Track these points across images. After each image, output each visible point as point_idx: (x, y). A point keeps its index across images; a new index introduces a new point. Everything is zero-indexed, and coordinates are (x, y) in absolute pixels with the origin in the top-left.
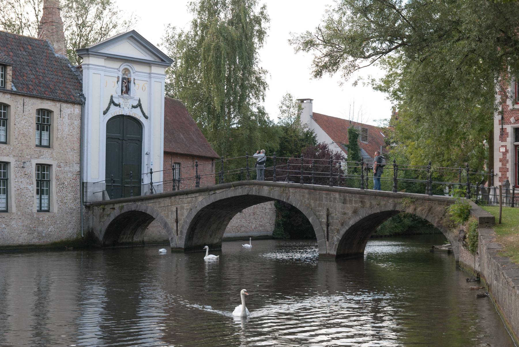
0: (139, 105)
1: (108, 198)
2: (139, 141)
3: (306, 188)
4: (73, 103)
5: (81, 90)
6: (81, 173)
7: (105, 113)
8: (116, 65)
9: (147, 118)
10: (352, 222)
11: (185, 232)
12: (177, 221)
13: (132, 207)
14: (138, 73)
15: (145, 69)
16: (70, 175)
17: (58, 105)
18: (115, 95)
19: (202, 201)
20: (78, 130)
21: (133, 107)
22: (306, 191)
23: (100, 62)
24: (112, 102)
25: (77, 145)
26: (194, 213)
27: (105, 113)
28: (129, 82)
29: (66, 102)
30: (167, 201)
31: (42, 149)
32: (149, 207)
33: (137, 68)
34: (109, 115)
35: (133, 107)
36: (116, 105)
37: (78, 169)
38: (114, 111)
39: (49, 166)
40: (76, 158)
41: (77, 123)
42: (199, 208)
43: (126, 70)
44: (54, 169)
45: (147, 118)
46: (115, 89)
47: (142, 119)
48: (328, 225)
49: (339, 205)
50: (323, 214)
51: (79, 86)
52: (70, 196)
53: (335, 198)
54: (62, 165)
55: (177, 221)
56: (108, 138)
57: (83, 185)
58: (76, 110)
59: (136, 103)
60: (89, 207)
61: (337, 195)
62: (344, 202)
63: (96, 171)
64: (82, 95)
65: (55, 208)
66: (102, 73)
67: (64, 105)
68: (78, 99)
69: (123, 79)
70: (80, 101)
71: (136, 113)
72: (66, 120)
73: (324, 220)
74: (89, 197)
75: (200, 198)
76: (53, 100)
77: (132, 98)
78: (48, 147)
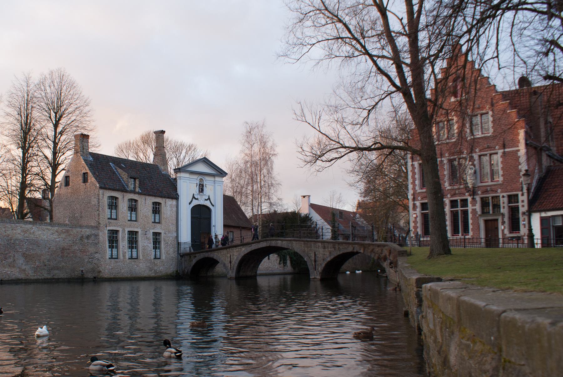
0: (209, 199)
1: (192, 251)
2: (209, 219)
4: (172, 198)
6: (177, 237)
7: (190, 204)
8: (195, 177)
11: (235, 268)
12: (230, 262)
13: (206, 255)
14: (208, 181)
15: (212, 179)
16: (171, 238)
17: (164, 199)
19: (245, 250)
20: (175, 213)
21: (206, 200)
22: (302, 243)
23: (187, 175)
24: (194, 197)
25: (175, 222)
27: (190, 204)
28: (203, 186)
32: (215, 255)
33: (207, 178)
35: (206, 200)
37: (176, 235)
38: (195, 202)
40: (175, 229)
41: (175, 209)
42: (243, 255)
44: (163, 235)
45: (213, 206)
46: (195, 190)
47: (211, 207)
49: (321, 250)
52: (172, 250)
53: (319, 246)
55: (230, 262)
56: (192, 218)
57: (179, 244)
58: (174, 202)
59: (207, 198)
60: (182, 256)
61: (320, 244)
62: (324, 248)
63: (186, 236)
64: (177, 194)
65: (163, 257)
66: (188, 181)
67: (167, 200)
69: (200, 184)
71: (208, 203)
72: (169, 208)
73: (313, 259)
74: (182, 250)
76: (161, 197)
78: (159, 223)
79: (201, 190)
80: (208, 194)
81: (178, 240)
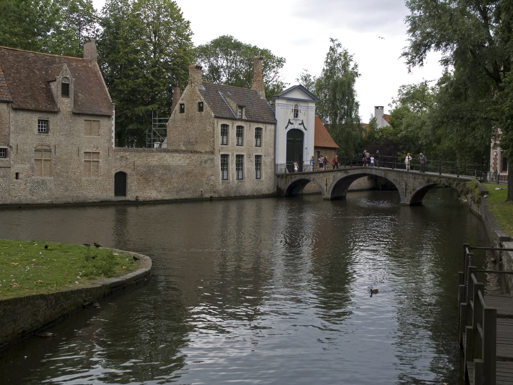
0: (303, 123)
1: (288, 172)
2: (301, 142)
3: (395, 171)
6: (275, 159)
9: (306, 130)
10: (418, 189)
11: (331, 190)
14: (302, 107)
17: (265, 125)
18: (291, 118)
20: (273, 137)
21: (300, 124)
23: (284, 102)
24: (289, 122)
25: (273, 145)
28: (297, 111)
29: (268, 123)
31: (258, 148)
33: (302, 104)
34: (288, 129)
35: (300, 124)
38: (290, 127)
39: (260, 156)
41: (273, 133)
43: (296, 105)
44: (263, 157)
45: (306, 130)
46: (291, 116)
47: (304, 131)
48: (406, 190)
49: (412, 180)
50: (404, 184)
51: (274, 115)
52: (270, 171)
53: (410, 177)
56: (288, 141)
57: (276, 165)
58: (272, 127)
59: (301, 122)
60: (278, 176)
61: (411, 175)
62: (415, 179)
63: (282, 159)
64: (275, 119)
66: (285, 107)
67: (267, 125)
69: (295, 110)
70: (275, 123)
71: (301, 128)
73: (404, 187)
74: (279, 172)
76: (263, 123)
79: (296, 115)
80: (301, 119)
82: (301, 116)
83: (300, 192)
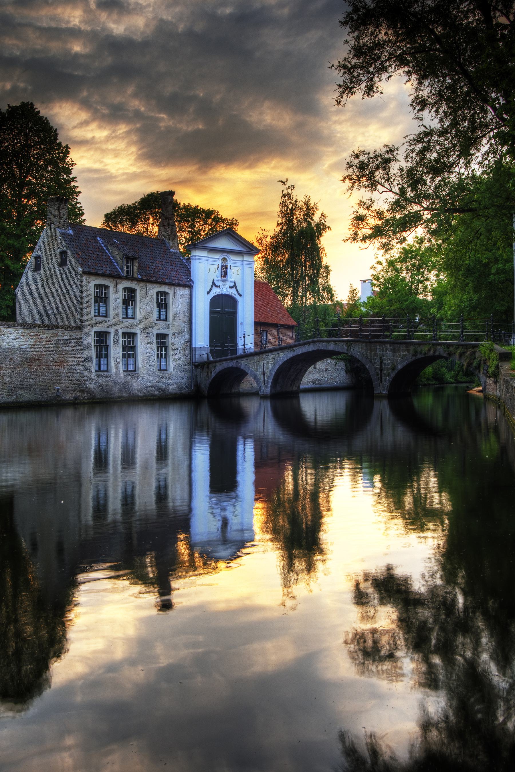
0: (235, 286)
1: (211, 358)
4: (184, 286)
5: (190, 276)
6: (190, 340)
7: (208, 293)
9: (240, 295)
14: (233, 261)
15: (240, 258)
17: (173, 288)
18: (216, 278)
19: (283, 357)
20: (187, 307)
21: (230, 287)
23: (205, 254)
24: (214, 284)
25: (187, 319)
26: (277, 367)
27: (208, 293)
28: (226, 267)
30: (257, 358)
32: (243, 364)
33: (232, 257)
34: (212, 295)
35: (230, 287)
36: (217, 286)
38: (215, 291)
41: (187, 301)
43: (224, 259)
45: (240, 295)
46: (215, 274)
47: (237, 297)
51: (189, 273)
54: (176, 334)
56: (211, 312)
57: (192, 350)
58: (187, 291)
59: (232, 284)
63: (202, 338)
64: (191, 280)
66: (206, 262)
67: (177, 288)
68: (188, 283)
69: (222, 266)
71: (233, 292)
72: (179, 300)
74: (197, 358)
75: (282, 355)
77: (228, 281)
80: (233, 280)
81: (191, 344)
82: (233, 276)
83: (234, 390)
